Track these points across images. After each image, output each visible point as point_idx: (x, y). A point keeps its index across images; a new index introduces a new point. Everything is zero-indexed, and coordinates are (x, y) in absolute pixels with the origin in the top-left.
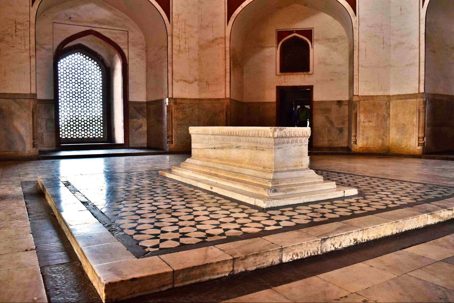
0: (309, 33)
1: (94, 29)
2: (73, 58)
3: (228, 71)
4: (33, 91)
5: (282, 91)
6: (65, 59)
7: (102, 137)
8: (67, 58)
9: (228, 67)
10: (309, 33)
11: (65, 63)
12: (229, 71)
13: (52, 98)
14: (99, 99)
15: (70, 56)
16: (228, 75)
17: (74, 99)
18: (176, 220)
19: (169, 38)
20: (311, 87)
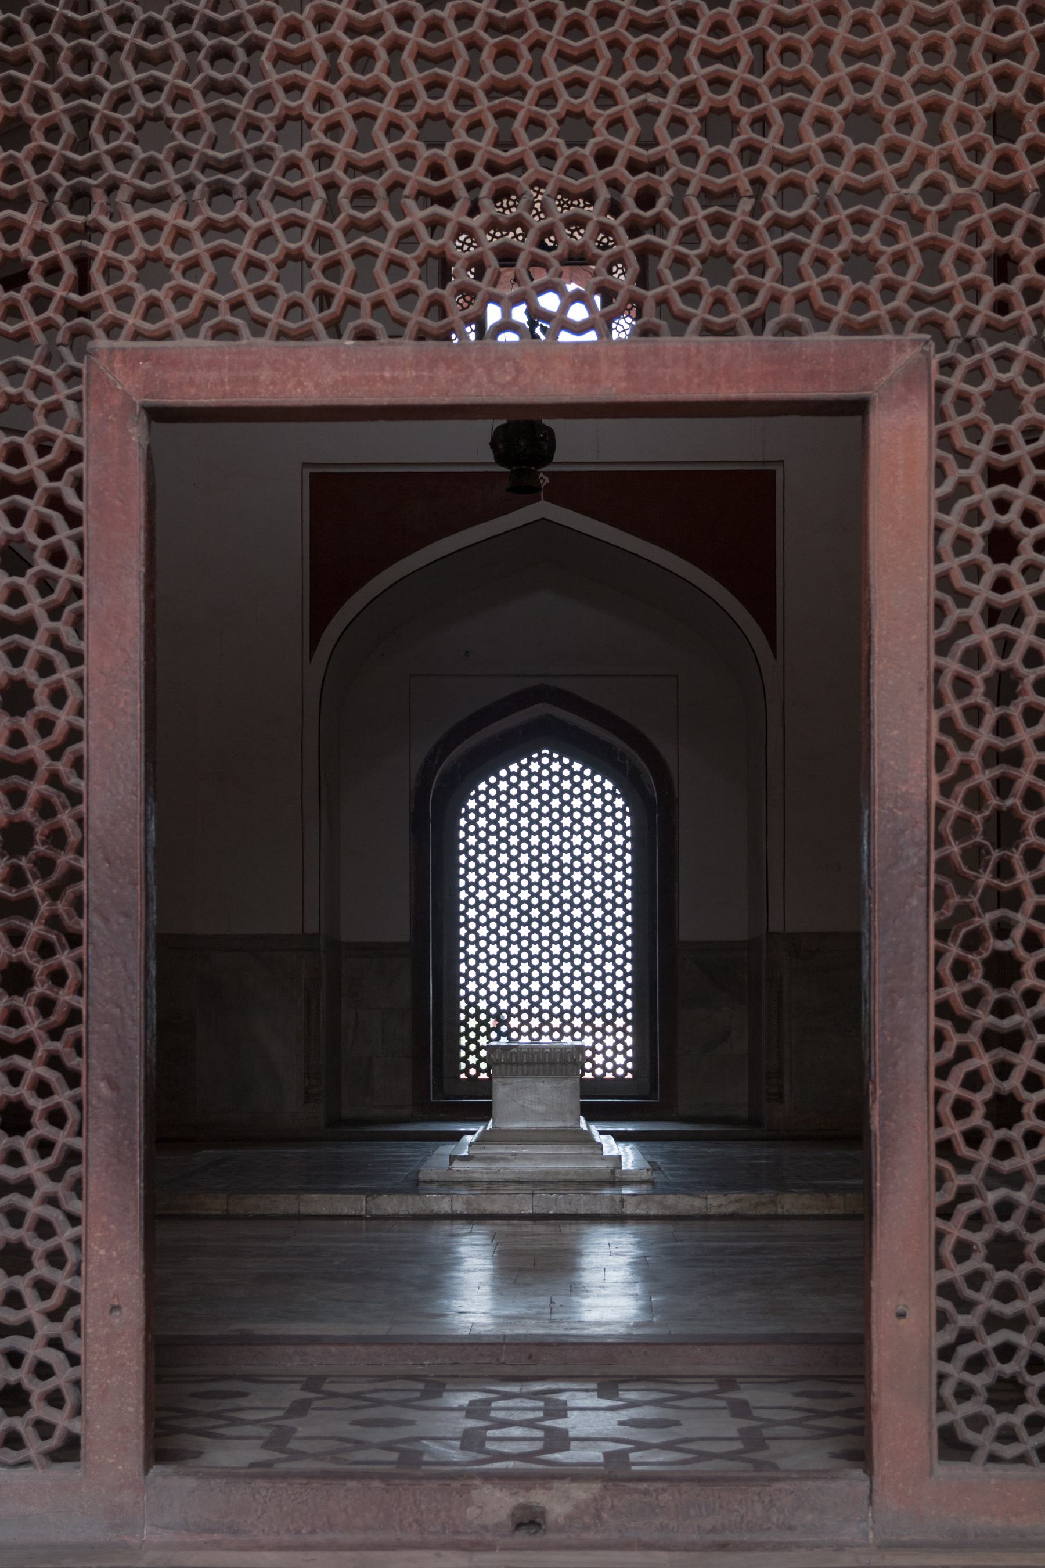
4: (312, 927)
7: (629, 1076)
13: (403, 934)
17: (524, 931)
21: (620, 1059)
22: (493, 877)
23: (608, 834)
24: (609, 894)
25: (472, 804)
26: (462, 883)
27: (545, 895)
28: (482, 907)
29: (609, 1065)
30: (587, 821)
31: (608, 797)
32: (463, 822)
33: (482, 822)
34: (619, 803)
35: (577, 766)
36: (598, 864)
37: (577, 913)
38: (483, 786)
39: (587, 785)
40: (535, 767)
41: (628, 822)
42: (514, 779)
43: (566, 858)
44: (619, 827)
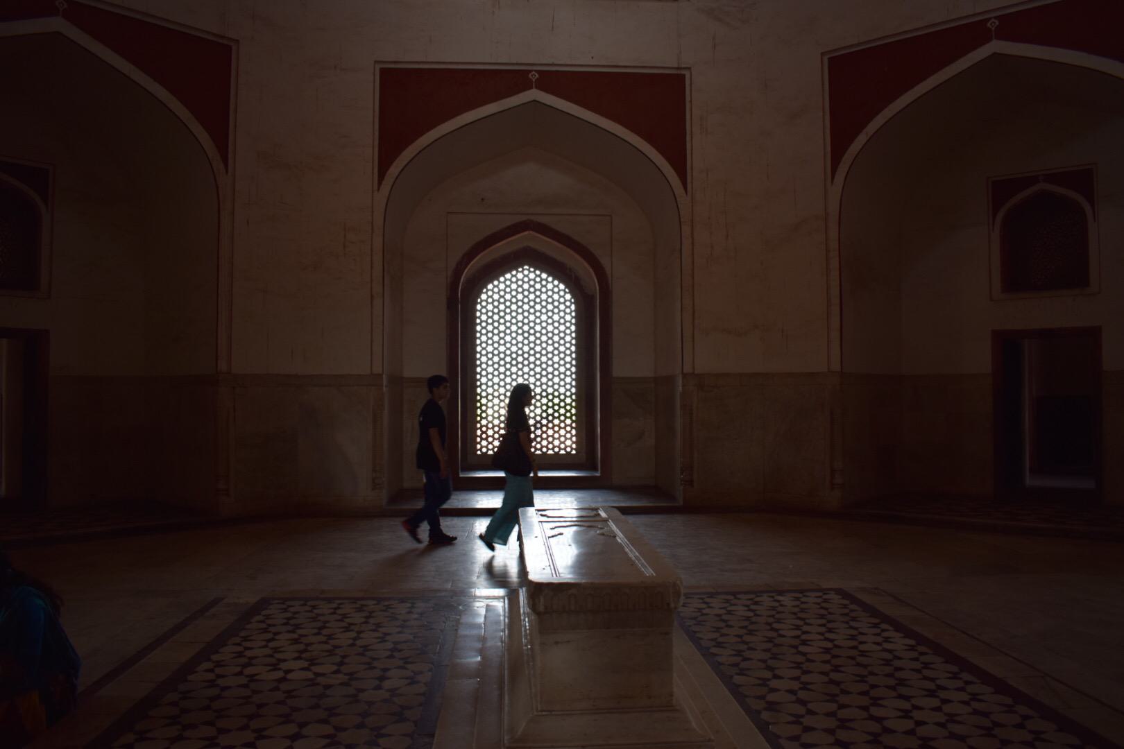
0: (1083, 180)
1: (532, 218)
2: (514, 279)
3: (836, 301)
4: (377, 369)
5: (1007, 345)
6: (496, 283)
8: (502, 279)
9: (835, 292)
10: (1083, 180)
11: (496, 290)
12: (838, 301)
14: (568, 366)
15: (508, 276)
16: (836, 310)
17: (514, 369)
18: (828, 635)
19: (686, 230)
20: (1093, 334)
21: (568, 443)
22: (496, 338)
23: (562, 314)
24: (562, 349)
25: (484, 297)
26: (478, 342)
27: (526, 349)
28: (490, 356)
29: (562, 446)
30: (550, 307)
31: (562, 293)
32: (479, 307)
33: (490, 307)
34: (568, 297)
35: (544, 276)
36: (556, 331)
37: (544, 359)
38: (490, 286)
39: (550, 286)
40: (520, 276)
41: (573, 307)
42: (508, 283)
43: (538, 328)
44: (568, 311)
